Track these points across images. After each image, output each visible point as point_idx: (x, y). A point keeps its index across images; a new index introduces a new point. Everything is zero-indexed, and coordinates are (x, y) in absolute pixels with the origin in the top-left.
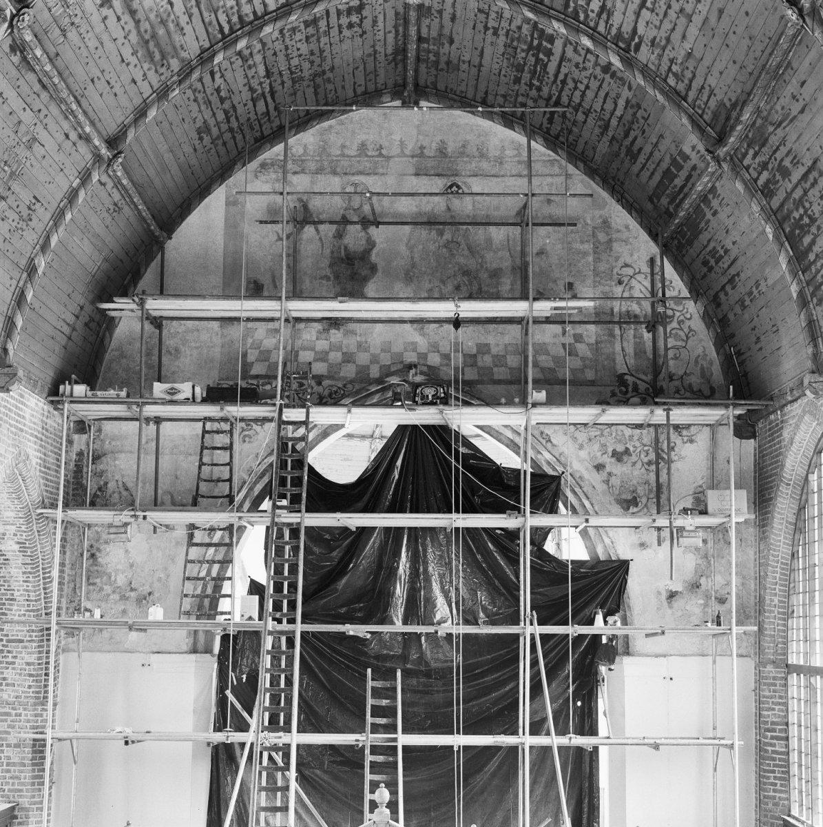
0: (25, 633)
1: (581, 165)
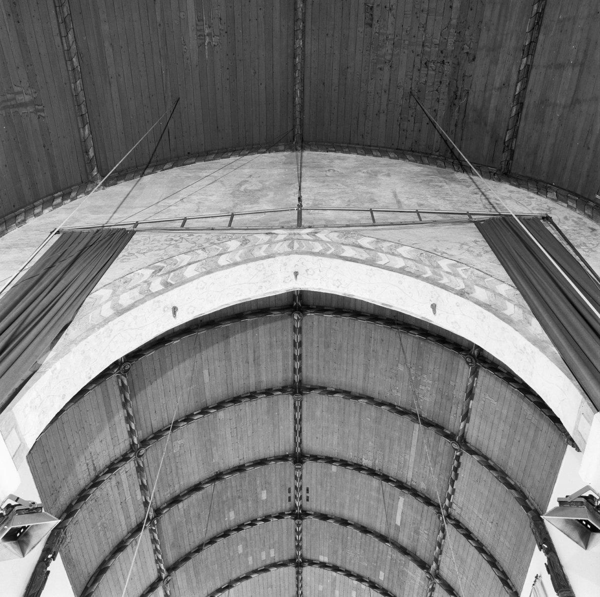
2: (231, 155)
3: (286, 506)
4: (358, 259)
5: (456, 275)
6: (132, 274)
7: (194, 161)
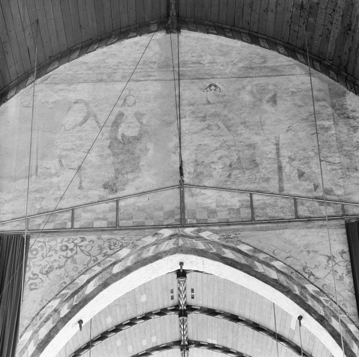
1: (317, 65)
2: (97, 48)
3: (169, 303)
4: (237, 263)
5: (319, 301)
6: (45, 309)
7: (57, 65)
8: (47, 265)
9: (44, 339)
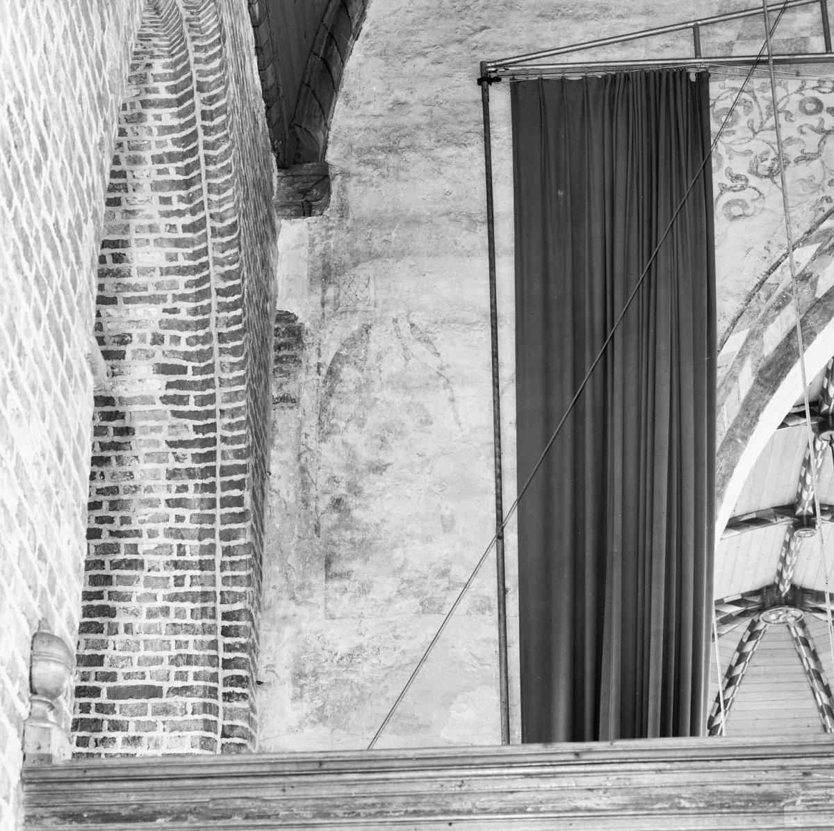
0: (166, 666)
6: (779, 270)
8: (767, 153)
9: (774, 358)
